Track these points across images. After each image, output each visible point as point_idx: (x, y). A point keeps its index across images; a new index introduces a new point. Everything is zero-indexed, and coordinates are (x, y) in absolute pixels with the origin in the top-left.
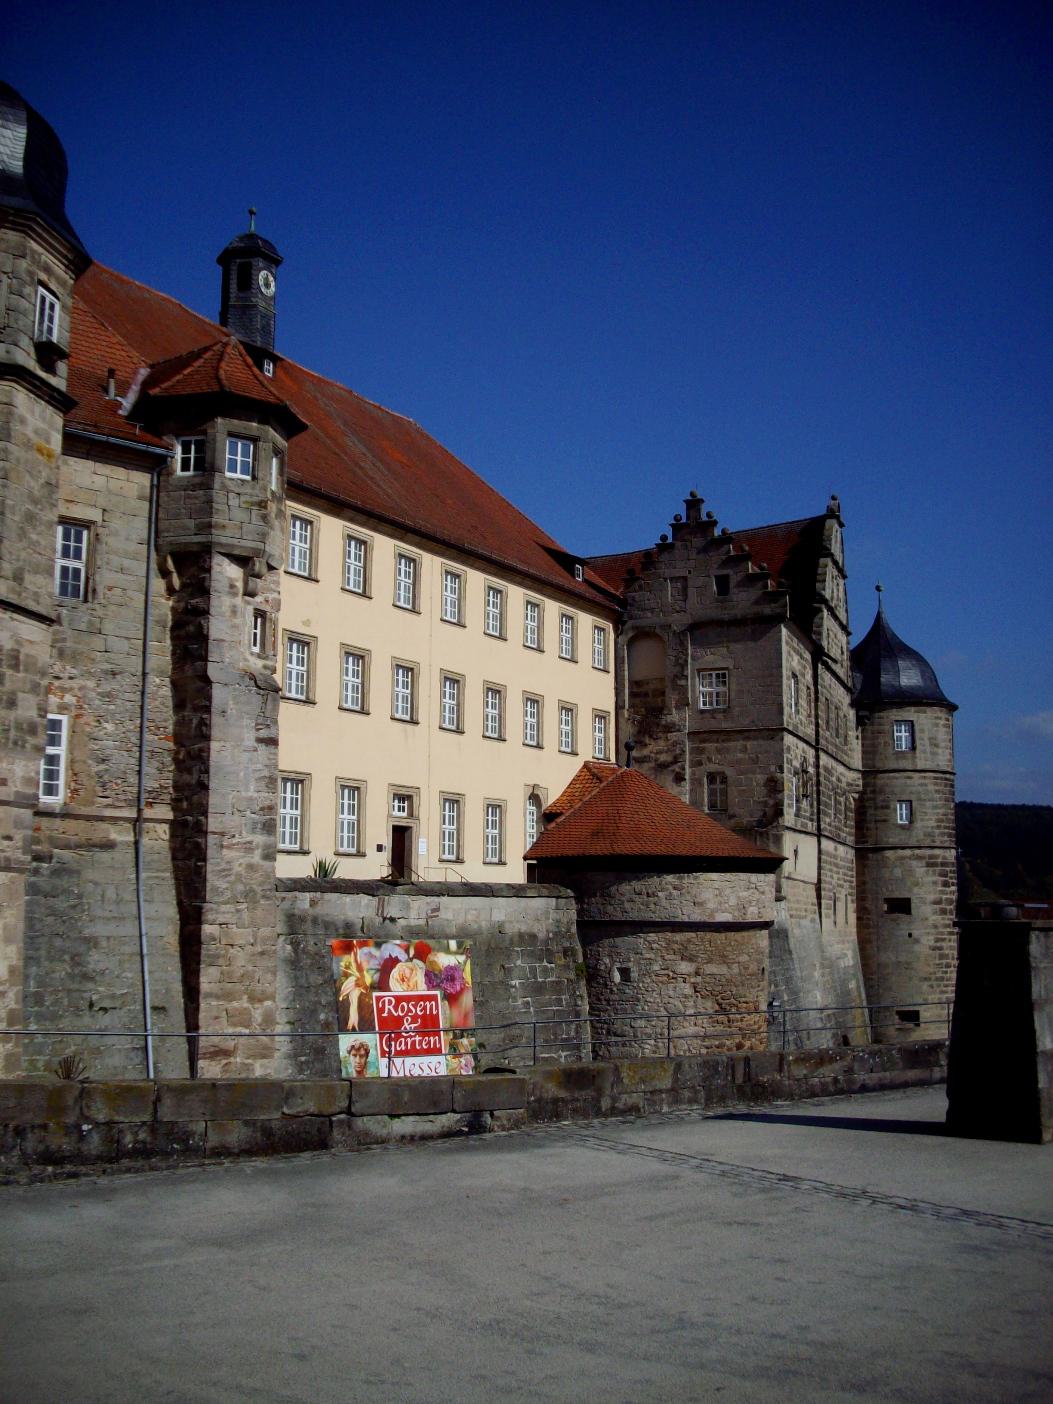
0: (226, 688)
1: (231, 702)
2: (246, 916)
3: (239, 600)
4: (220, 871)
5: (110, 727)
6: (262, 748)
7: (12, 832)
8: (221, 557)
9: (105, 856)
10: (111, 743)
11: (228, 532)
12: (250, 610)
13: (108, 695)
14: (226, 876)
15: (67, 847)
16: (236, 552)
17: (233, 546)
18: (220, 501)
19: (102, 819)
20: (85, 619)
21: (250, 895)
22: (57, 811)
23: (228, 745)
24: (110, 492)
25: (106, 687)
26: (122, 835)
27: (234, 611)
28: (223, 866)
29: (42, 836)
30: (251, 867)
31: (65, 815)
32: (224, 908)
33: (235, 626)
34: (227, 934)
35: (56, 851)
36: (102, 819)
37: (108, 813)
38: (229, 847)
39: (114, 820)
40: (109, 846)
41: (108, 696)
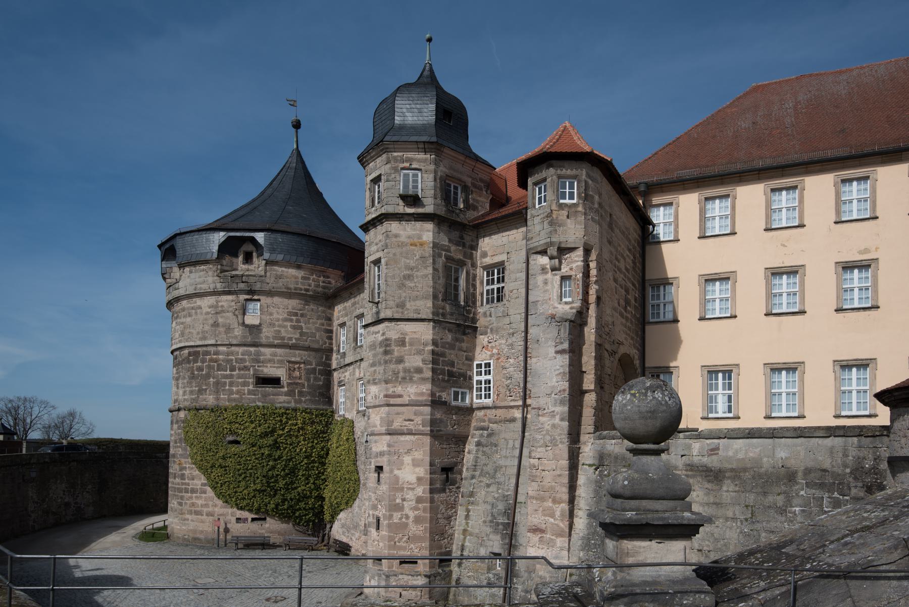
2: (550, 453)
3: (549, 275)
5: (512, 361)
6: (559, 356)
8: (535, 256)
10: (512, 369)
11: (534, 240)
12: (558, 278)
13: (512, 345)
15: (496, 422)
16: (539, 249)
17: (536, 247)
19: (512, 407)
25: (510, 341)
26: (518, 414)
28: (540, 426)
29: (486, 419)
30: (554, 426)
31: (495, 407)
32: (539, 450)
33: (546, 291)
34: (541, 464)
37: (512, 404)
38: (543, 415)
40: (513, 420)
41: (511, 346)
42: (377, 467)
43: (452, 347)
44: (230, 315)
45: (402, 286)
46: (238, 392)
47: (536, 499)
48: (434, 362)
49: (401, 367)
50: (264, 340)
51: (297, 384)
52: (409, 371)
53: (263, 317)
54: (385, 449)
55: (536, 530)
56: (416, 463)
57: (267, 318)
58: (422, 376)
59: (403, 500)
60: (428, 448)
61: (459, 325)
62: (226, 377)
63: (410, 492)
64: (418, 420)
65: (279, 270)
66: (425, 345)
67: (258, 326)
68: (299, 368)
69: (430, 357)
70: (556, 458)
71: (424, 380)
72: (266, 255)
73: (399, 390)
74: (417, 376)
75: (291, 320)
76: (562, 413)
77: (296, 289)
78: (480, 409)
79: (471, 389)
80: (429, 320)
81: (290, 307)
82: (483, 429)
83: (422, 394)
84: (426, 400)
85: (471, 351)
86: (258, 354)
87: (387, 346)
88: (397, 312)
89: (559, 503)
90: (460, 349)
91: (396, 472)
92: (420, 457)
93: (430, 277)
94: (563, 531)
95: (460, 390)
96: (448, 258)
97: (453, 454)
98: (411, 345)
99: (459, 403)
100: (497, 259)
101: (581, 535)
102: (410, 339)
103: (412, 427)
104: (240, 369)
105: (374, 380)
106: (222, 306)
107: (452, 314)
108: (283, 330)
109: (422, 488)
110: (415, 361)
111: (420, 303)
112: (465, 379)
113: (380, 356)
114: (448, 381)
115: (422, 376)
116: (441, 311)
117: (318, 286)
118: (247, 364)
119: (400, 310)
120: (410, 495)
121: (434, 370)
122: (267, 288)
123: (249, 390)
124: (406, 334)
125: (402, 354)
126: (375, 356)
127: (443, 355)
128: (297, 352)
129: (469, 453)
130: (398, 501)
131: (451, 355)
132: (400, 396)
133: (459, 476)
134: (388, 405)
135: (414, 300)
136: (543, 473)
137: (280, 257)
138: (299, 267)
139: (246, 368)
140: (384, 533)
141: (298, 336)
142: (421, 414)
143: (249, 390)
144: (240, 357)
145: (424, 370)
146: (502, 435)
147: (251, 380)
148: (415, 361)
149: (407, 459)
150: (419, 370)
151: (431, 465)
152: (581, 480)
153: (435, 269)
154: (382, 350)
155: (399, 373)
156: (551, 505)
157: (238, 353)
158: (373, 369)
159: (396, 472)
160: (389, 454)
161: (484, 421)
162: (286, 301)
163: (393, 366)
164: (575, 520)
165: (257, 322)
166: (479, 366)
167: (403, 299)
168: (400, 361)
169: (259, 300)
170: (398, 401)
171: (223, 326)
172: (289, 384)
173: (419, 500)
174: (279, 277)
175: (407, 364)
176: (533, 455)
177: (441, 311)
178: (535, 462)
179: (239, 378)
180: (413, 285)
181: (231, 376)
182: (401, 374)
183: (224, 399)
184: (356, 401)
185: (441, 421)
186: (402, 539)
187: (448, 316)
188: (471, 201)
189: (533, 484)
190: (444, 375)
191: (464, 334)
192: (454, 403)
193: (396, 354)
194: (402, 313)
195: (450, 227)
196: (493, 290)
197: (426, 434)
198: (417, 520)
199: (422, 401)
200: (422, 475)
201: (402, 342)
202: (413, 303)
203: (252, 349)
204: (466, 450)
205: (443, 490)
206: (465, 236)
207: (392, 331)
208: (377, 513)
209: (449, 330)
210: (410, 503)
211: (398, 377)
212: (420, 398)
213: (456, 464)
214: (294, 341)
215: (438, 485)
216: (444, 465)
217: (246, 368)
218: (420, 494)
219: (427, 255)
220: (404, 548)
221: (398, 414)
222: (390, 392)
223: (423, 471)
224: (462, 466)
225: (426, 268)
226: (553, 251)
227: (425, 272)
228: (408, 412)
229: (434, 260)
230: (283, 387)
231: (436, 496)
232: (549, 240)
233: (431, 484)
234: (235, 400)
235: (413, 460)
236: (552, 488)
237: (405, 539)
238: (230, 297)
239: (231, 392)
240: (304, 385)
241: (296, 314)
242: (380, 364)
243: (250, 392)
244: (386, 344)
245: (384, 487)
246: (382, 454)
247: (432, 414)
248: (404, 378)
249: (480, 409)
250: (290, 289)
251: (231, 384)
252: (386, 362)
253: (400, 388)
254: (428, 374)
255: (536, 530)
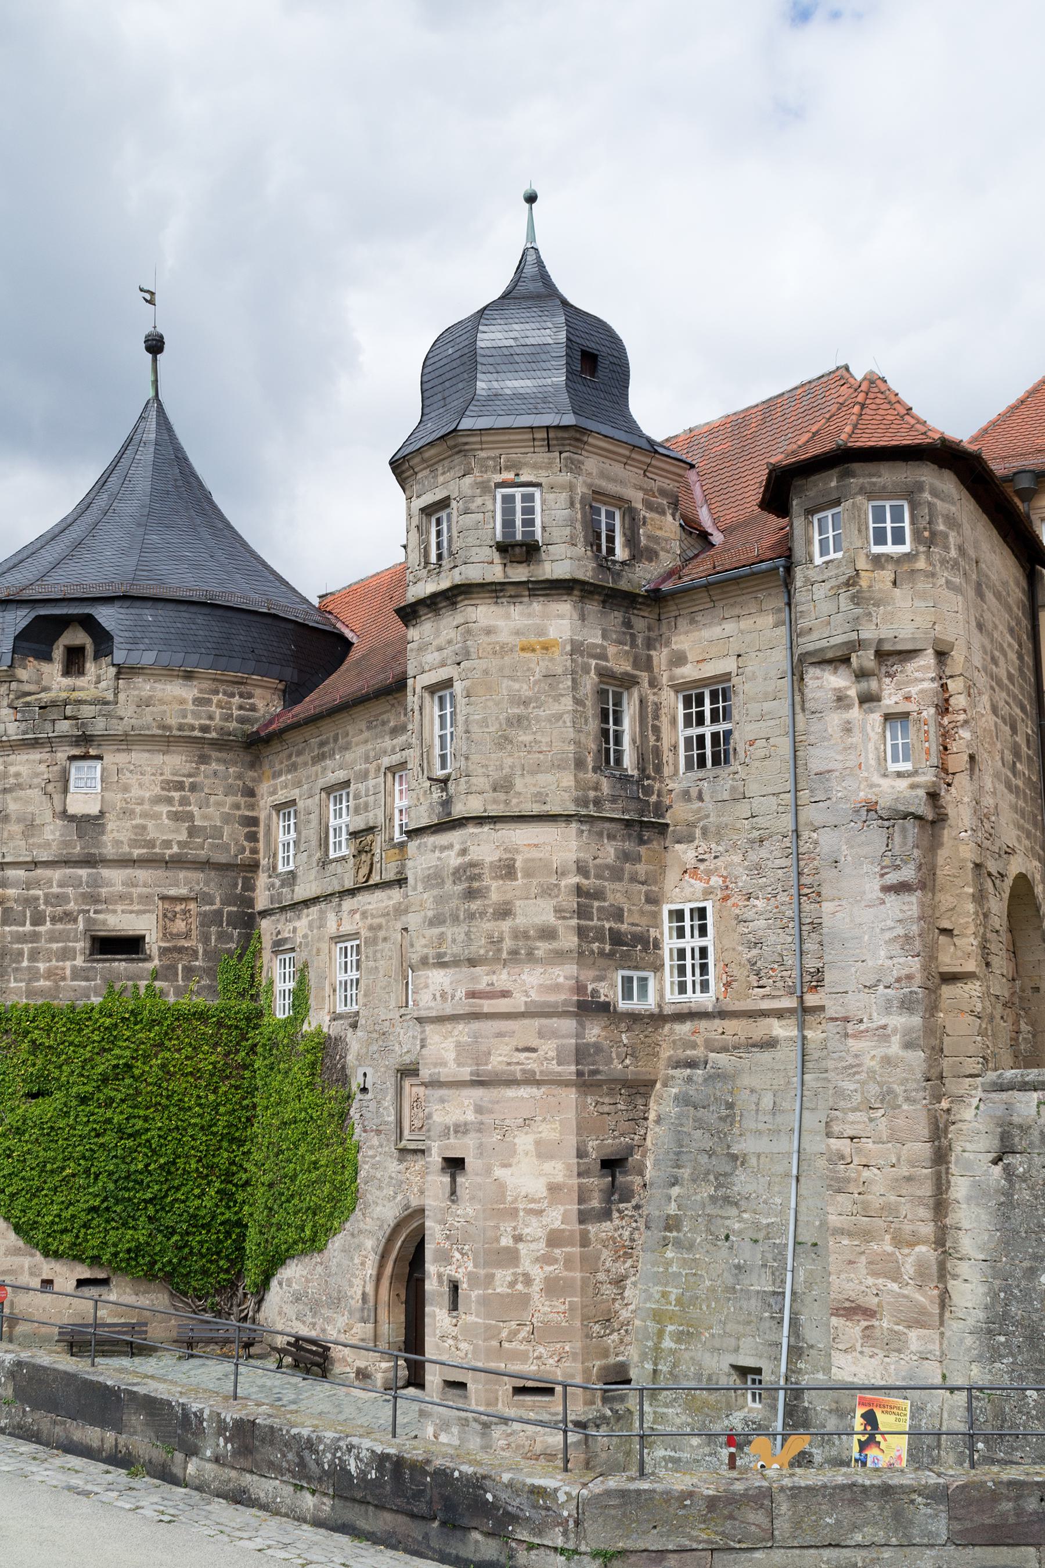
0: (837, 832)
1: (844, 847)
4: (845, 1068)
7: (534, 1043)
9: (765, 1057)
14: (855, 1073)
15: (724, 1049)
18: (803, 600)
19: (764, 1014)
20: (727, 786)
21: (887, 1097)
22: (710, 1010)
23: (844, 903)
24: (742, 632)
27: (847, 729)
29: (699, 1040)
31: (722, 1014)
35: (712, 1055)
36: (764, 1014)
39: (780, 1014)
42: (446, 1160)
43: (617, 874)
44: (35, 793)
45: (504, 741)
46: (49, 974)
47: (850, 1234)
48: (582, 912)
49: (506, 925)
50: (109, 851)
51: (180, 950)
52: (526, 936)
53: (109, 795)
54: (470, 1116)
55: (853, 1310)
56: (544, 1152)
57: (116, 798)
58: (555, 945)
59: (518, 1239)
60: (571, 1115)
61: (628, 824)
62: (22, 938)
63: (534, 1220)
64: (548, 1048)
65: (144, 687)
66: (561, 873)
67: (97, 818)
68: (185, 912)
69: (572, 903)
70: (896, 1138)
71: (560, 956)
72: (119, 656)
73: (502, 979)
74: (542, 948)
75: (169, 801)
76: (907, 1031)
77: (181, 728)
78: (681, 1017)
79: (658, 968)
80: (568, 818)
81: (167, 770)
82: (691, 1064)
83: (556, 988)
84: (565, 1003)
85: (655, 883)
86: (96, 882)
87: (472, 878)
88: (495, 801)
89: (912, 1245)
90: (634, 879)
91: (499, 1172)
92: (554, 1136)
93: (568, 718)
94: (923, 1311)
95: (635, 974)
96: (605, 675)
97: (624, 1126)
98: (528, 874)
99: (634, 1005)
100: (711, 669)
101: (971, 1322)
102: (526, 861)
103: (532, 1066)
104: (54, 920)
105: (440, 956)
106: (17, 775)
107: (614, 799)
108: (150, 824)
109: (562, 1208)
110: (536, 912)
111: (545, 779)
112: (645, 949)
113: (454, 903)
114: (611, 955)
115: (555, 945)
116: (592, 794)
117: (228, 718)
118: (72, 906)
119: (502, 796)
120: (534, 1228)
121: (581, 932)
122: (118, 728)
123: (74, 968)
124: (517, 851)
125: (508, 896)
126: (439, 900)
127: (599, 895)
128: (182, 875)
129: (658, 1121)
130: (506, 1241)
131: (615, 894)
132: (505, 994)
133: (638, 1180)
134: (476, 1016)
135: (533, 773)
136: (866, 1174)
137: (148, 658)
138: (189, 676)
139: (69, 917)
140: (472, 1319)
141: (183, 836)
142: (555, 1034)
143: (74, 968)
144: (55, 890)
145: (561, 931)
146: (746, 1080)
147: (79, 945)
148: (536, 912)
149: (524, 1141)
150: (548, 934)
151: (581, 1154)
152: (960, 1188)
153: (578, 702)
154: (460, 888)
155: (501, 940)
156: (889, 1249)
157: (49, 882)
158: (436, 931)
159: (499, 1172)
160: (479, 1131)
161: (694, 1046)
162: (159, 759)
163: (488, 926)
164: (951, 1284)
165: (94, 810)
166: (679, 915)
167: (507, 770)
168: (504, 912)
169: (99, 758)
170: (502, 1005)
171: (19, 821)
172: (164, 952)
173: (554, 1239)
174: (146, 703)
175: (520, 921)
176: (836, 1128)
177: (592, 794)
178: (844, 1146)
179: (52, 939)
180: (526, 738)
181: (35, 937)
182: (508, 944)
183: (17, 992)
184: (328, 990)
185: (598, 1048)
186: (515, 1333)
187: (607, 805)
188: (643, 541)
189: (840, 1198)
190: (602, 940)
191: (642, 842)
192: (623, 1006)
193: (494, 896)
194: (507, 803)
195: (604, 602)
196: (701, 738)
197: (566, 1084)
198: (553, 1288)
199: (555, 1004)
200: (560, 1179)
201: (507, 870)
202: (529, 779)
203: (83, 872)
204: (652, 1116)
205: (606, 1215)
206: (634, 620)
207: (485, 846)
208: (450, 1271)
209: (609, 837)
210: (533, 1246)
211: (499, 950)
212: (552, 998)
213: (630, 1150)
214: (175, 849)
215: (595, 1203)
216: (608, 1153)
217: (69, 917)
218: (557, 1224)
219: (559, 670)
220: (523, 1357)
221: (500, 1035)
222: (482, 986)
223: (560, 1169)
224: (644, 1156)
225: (557, 698)
226: (866, 659)
227: (555, 708)
228: (526, 1031)
229: (574, 680)
230: (149, 959)
231: (592, 1229)
232: (854, 636)
233: (581, 1201)
234: (41, 993)
235: (538, 1143)
236: (888, 1209)
237: (524, 1333)
238: (35, 755)
239: (34, 975)
240: (195, 952)
241: (180, 786)
242: (455, 919)
243: (76, 974)
244: (469, 876)
245: (467, 1209)
246: (461, 1129)
247: (579, 1035)
248: (514, 953)
249: (681, 1017)
250: (168, 728)
251: (34, 956)
252: (471, 916)
253: (504, 976)
254: (569, 941)
255: (853, 1310)
